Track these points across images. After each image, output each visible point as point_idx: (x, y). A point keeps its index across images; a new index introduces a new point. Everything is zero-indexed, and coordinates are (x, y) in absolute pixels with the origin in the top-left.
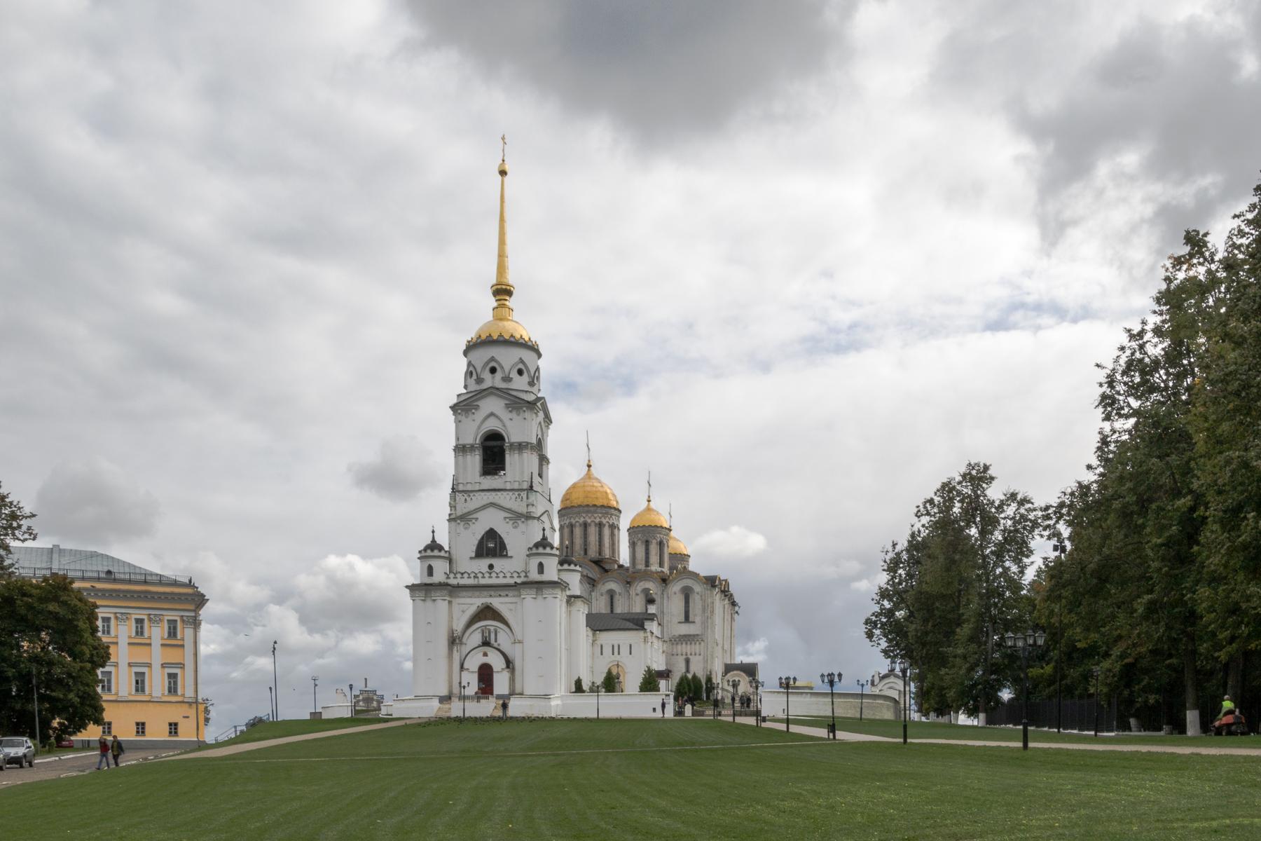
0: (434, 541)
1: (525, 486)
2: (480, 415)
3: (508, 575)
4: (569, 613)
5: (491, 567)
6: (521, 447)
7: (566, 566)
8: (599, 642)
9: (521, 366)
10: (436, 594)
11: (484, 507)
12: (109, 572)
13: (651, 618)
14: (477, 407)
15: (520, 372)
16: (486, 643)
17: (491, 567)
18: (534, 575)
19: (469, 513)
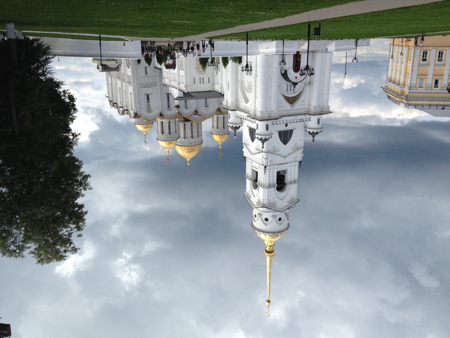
0: (314, 137)
1: (267, 168)
2: (288, 198)
3: (281, 122)
4: (237, 101)
5: (286, 125)
6: (270, 186)
7: (238, 126)
8: (211, 84)
9: (266, 222)
10: (318, 110)
11: (288, 155)
12: (443, 109)
13: (179, 98)
14: (289, 202)
15: (266, 220)
16: (295, 84)
17: (286, 125)
18: (269, 123)
19: (295, 151)
